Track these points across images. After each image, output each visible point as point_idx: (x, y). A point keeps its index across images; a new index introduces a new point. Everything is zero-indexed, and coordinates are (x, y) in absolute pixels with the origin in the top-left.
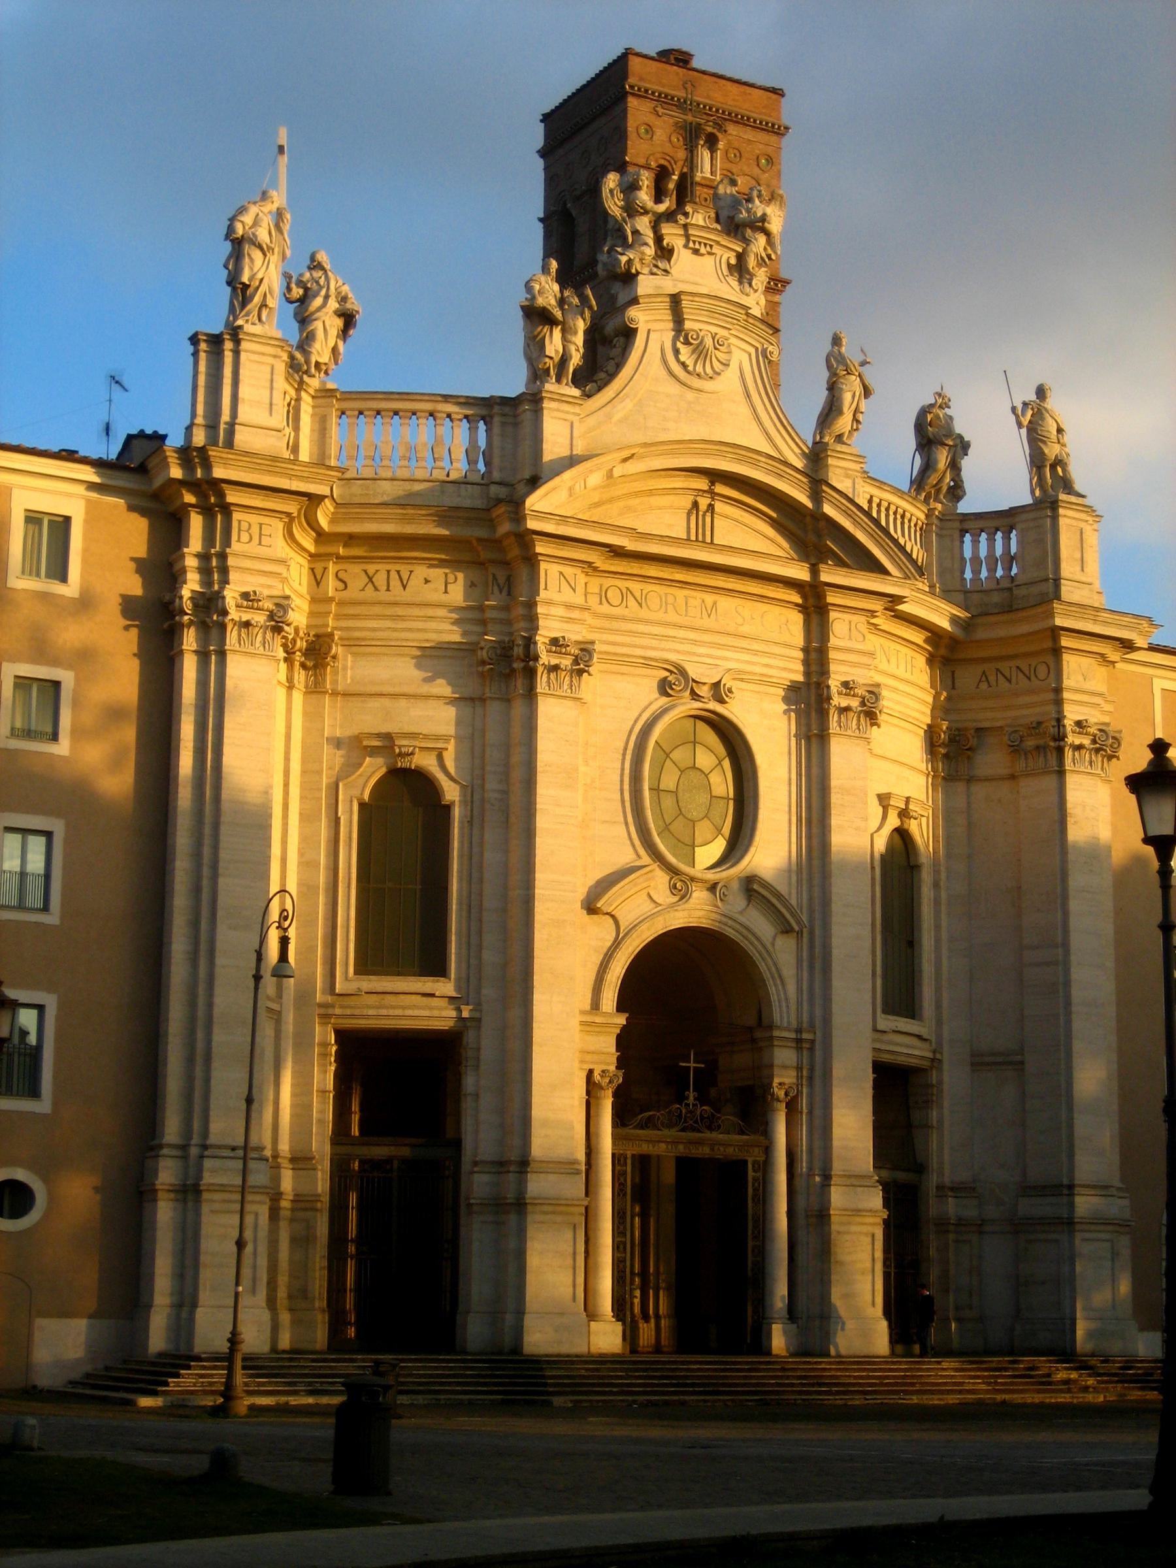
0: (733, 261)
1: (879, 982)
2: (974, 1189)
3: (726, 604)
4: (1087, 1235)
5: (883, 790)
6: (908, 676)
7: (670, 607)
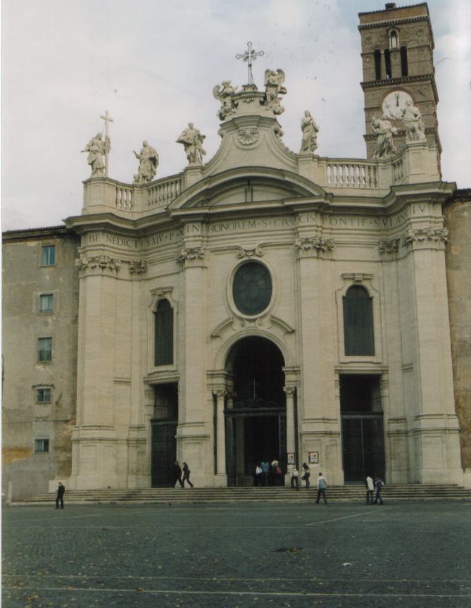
0: (262, 99)
1: (342, 346)
2: (405, 419)
3: (258, 221)
4: (427, 435)
5: (344, 272)
6: (358, 227)
7: (237, 228)
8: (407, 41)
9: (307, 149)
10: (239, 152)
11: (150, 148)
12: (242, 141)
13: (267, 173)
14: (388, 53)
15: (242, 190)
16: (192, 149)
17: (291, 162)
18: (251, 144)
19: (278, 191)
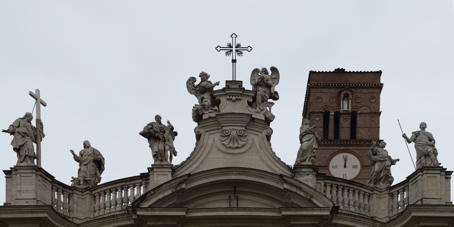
8: (359, 105)
9: (305, 160)
10: (221, 155)
11: (94, 150)
12: (225, 143)
13: (262, 177)
14: (337, 115)
15: (226, 197)
16: (161, 146)
17: (288, 173)
18: (237, 148)
19: (268, 202)
